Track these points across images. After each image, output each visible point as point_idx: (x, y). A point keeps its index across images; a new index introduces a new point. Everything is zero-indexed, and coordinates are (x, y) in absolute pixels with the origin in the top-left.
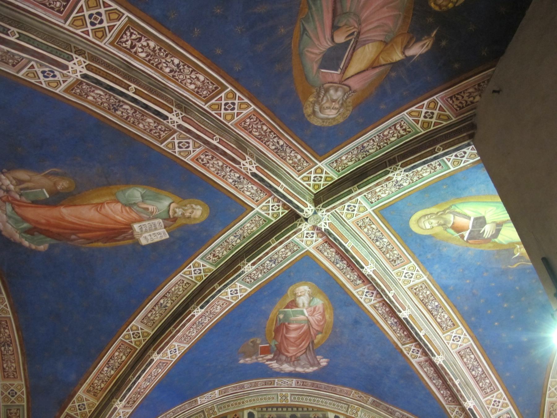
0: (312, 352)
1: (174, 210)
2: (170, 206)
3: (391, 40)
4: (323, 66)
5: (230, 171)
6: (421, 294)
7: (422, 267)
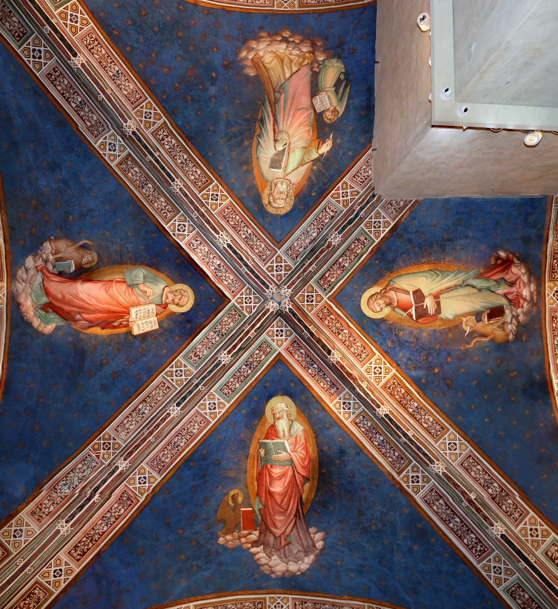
0: (303, 521)
1: (166, 294)
2: (164, 289)
3: (309, 145)
4: (271, 167)
5: (213, 258)
6: (396, 393)
7: (388, 358)
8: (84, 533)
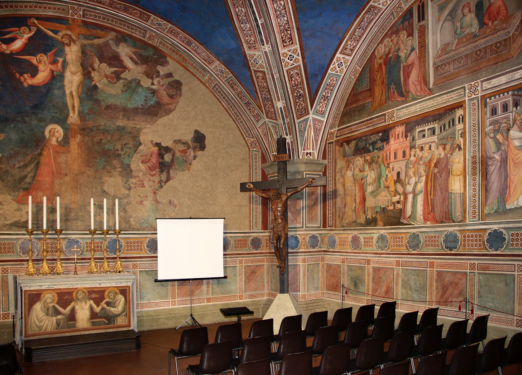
8: (279, 33)
